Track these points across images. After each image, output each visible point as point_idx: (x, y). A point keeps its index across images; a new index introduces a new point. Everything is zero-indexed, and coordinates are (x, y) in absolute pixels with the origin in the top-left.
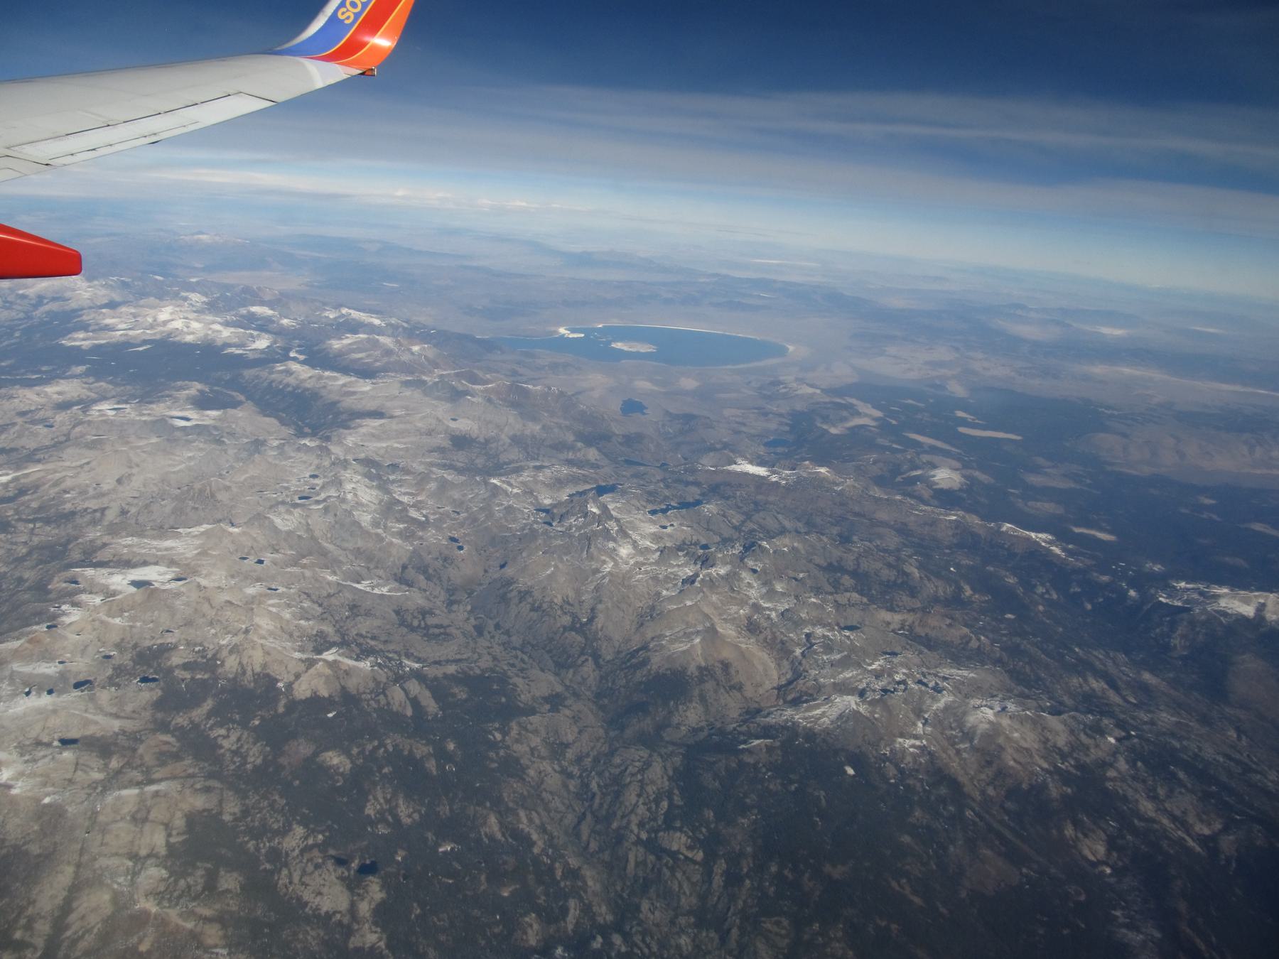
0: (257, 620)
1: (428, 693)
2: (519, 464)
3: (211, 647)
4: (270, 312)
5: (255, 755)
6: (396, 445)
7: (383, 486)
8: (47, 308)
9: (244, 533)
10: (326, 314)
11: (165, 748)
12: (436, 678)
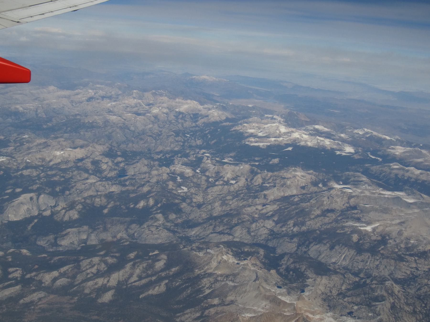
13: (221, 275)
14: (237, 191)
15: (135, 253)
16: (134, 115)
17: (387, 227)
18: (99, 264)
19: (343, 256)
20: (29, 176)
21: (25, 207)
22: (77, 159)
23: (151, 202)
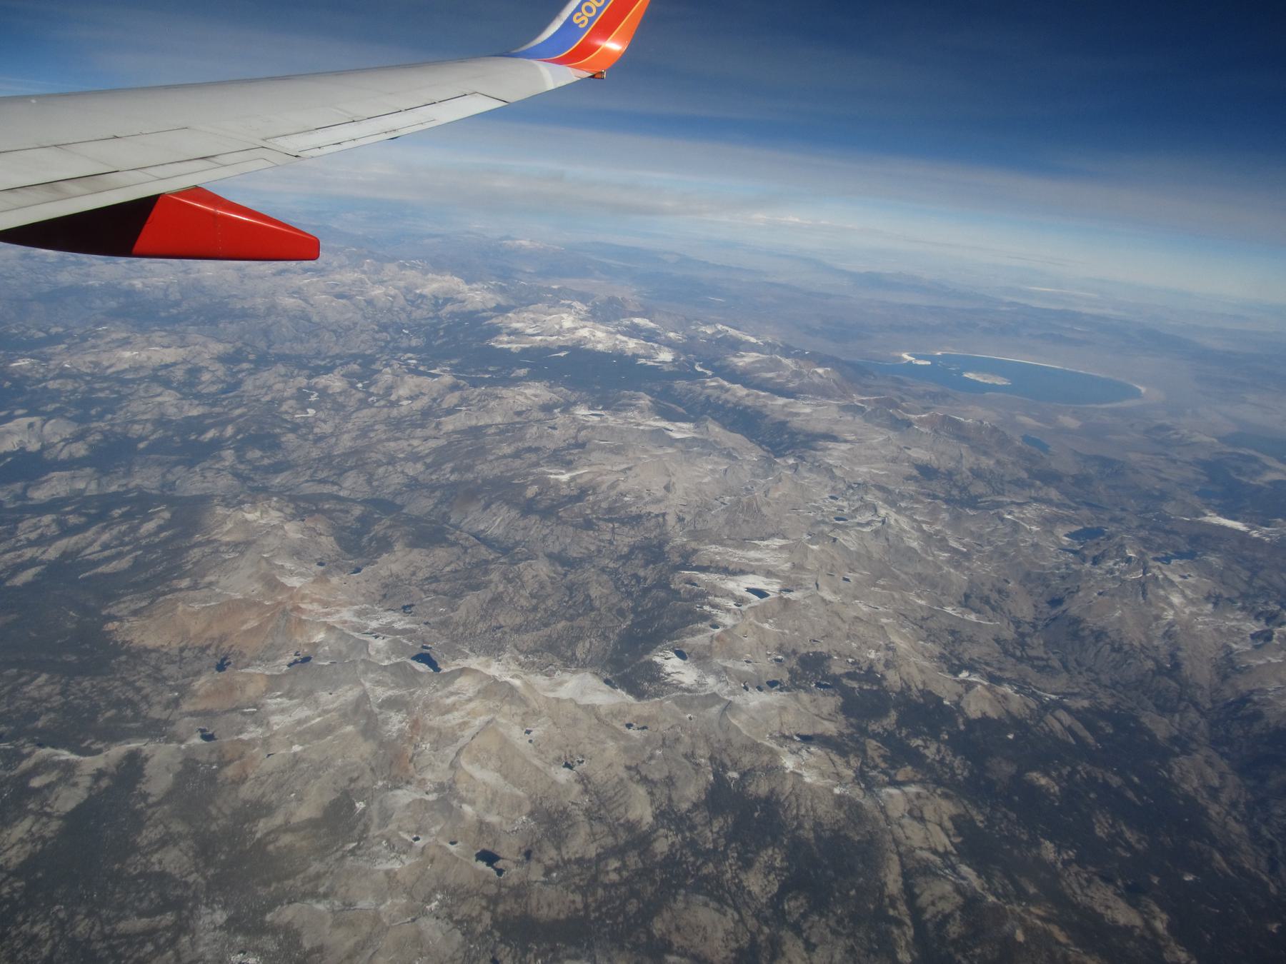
3: (862, 660)
4: (652, 325)
8: (449, 308)
9: (823, 551)
12: (1078, 711)
13: (227, 544)
14: (402, 417)
15: (124, 509)
16: (330, 298)
17: (601, 475)
18: (48, 526)
19: (499, 520)
20: (58, 390)
21: (16, 439)
22: (163, 363)
23: (229, 431)
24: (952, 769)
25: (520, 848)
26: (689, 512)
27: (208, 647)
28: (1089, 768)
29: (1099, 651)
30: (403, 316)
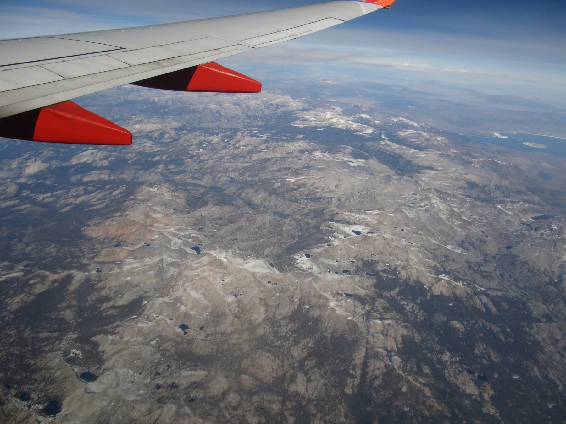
0: (410, 256)
1: (491, 303)
2: (500, 199)
3: (393, 265)
4: (369, 117)
5: (421, 316)
6: (444, 184)
7: (445, 202)
8: (281, 109)
9: (395, 217)
10: (393, 119)
11: (384, 305)
12: (493, 297)
13: (140, 200)
15: (110, 186)
17: (310, 180)
18: (81, 191)
23: (165, 157)
24: (416, 316)
25: (199, 325)
26: (344, 197)
27: (115, 238)
28: (484, 322)
29: (522, 271)
30: (260, 113)
